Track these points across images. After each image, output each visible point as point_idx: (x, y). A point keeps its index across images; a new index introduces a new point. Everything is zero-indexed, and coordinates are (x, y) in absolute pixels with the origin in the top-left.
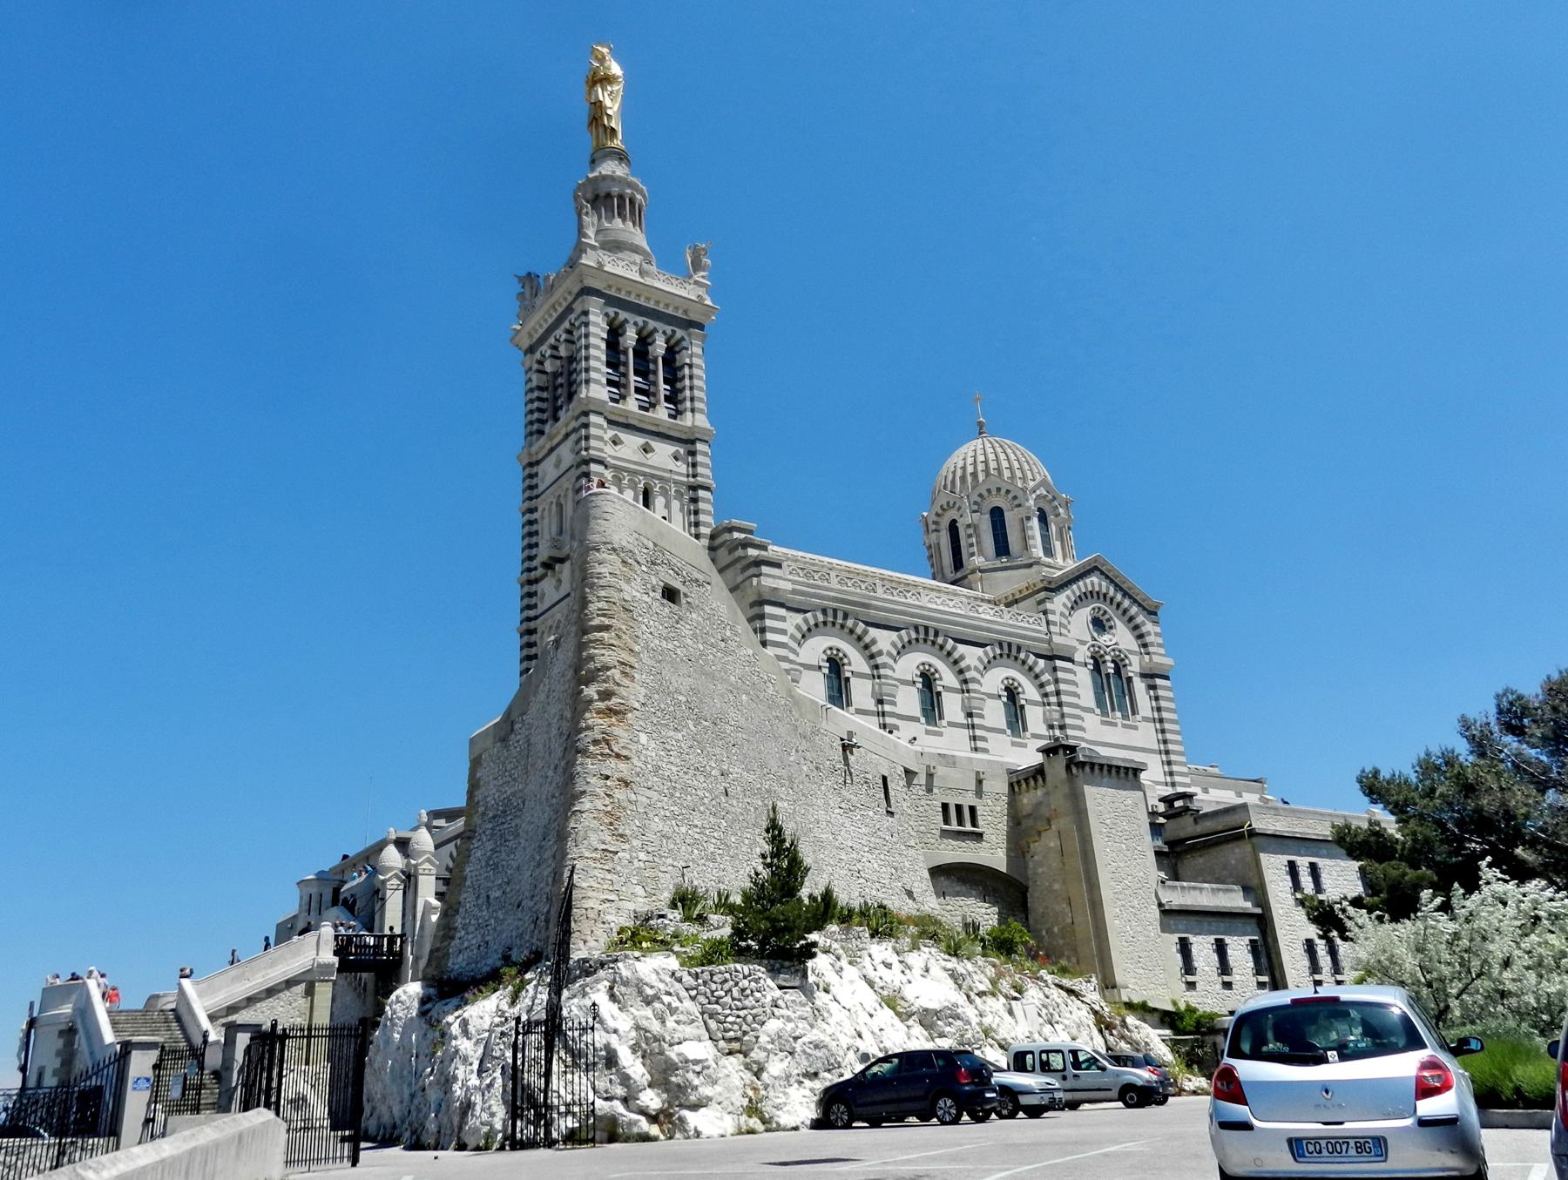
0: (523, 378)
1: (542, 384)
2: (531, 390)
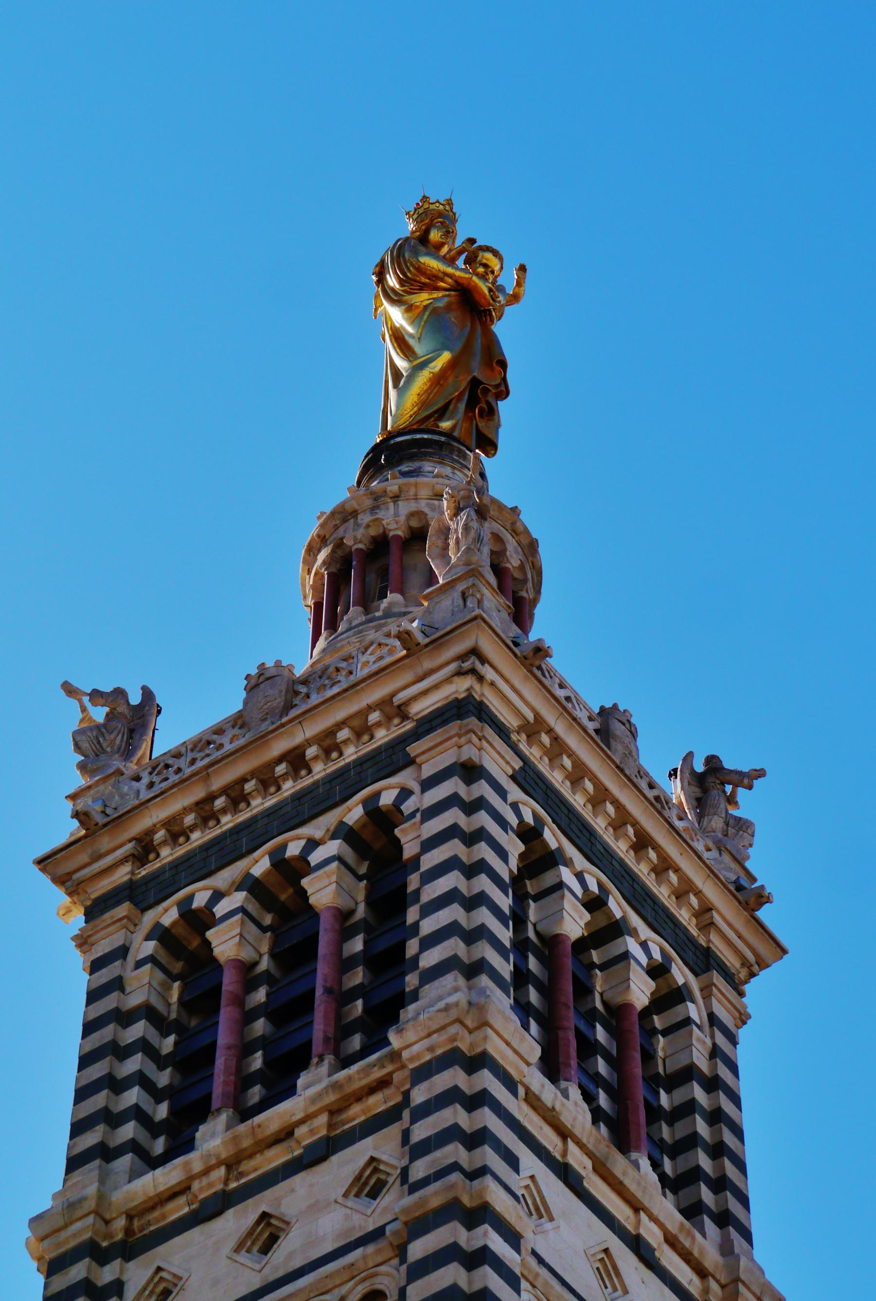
1: (160, 1007)
2: (124, 1018)
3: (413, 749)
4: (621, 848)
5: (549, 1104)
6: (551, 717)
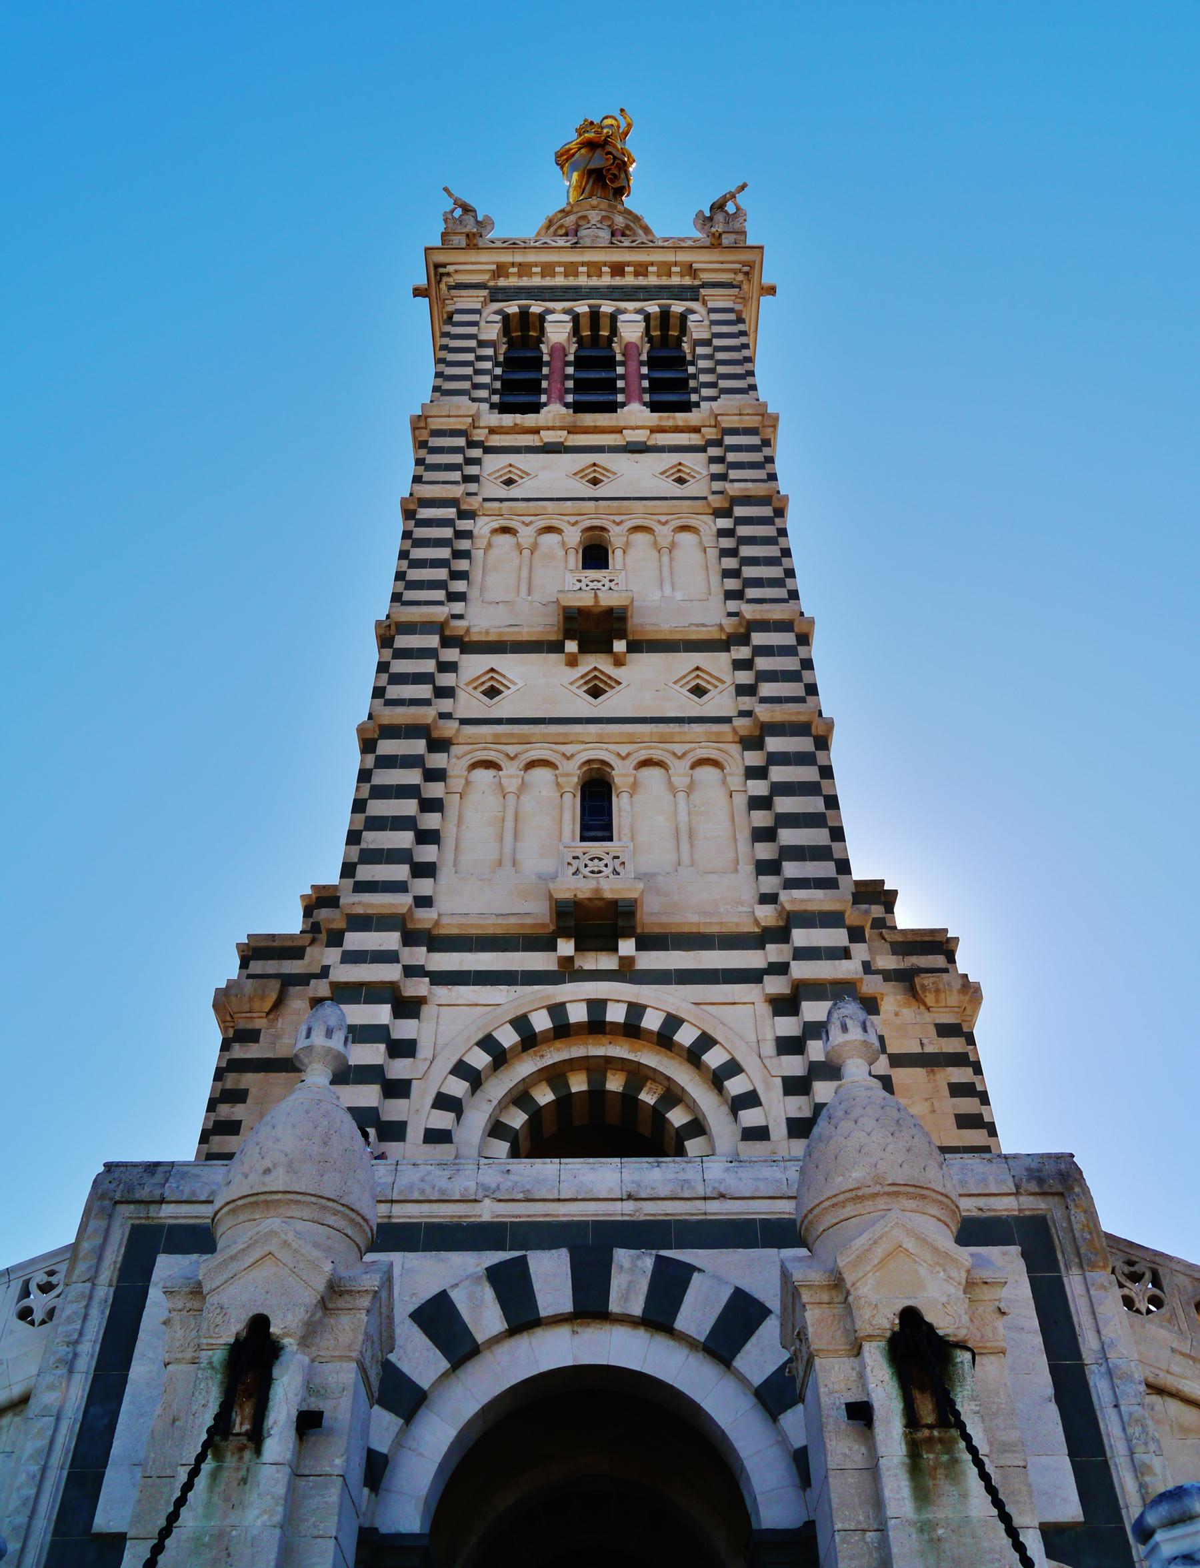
4: (606, 280)
5: (511, 424)
6: (506, 258)
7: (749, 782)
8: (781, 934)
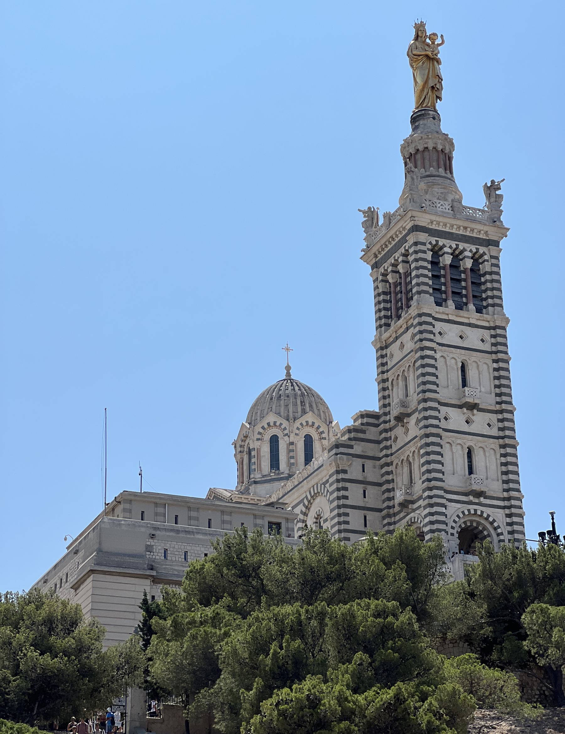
0: (372, 286)
1: (386, 290)
2: (379, 295)
3: (407, 238)
7: (502, 458)
8: (509, 499)
